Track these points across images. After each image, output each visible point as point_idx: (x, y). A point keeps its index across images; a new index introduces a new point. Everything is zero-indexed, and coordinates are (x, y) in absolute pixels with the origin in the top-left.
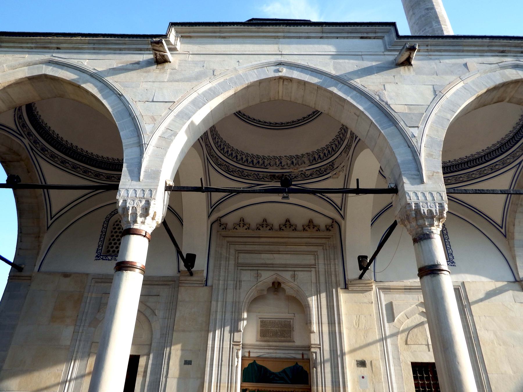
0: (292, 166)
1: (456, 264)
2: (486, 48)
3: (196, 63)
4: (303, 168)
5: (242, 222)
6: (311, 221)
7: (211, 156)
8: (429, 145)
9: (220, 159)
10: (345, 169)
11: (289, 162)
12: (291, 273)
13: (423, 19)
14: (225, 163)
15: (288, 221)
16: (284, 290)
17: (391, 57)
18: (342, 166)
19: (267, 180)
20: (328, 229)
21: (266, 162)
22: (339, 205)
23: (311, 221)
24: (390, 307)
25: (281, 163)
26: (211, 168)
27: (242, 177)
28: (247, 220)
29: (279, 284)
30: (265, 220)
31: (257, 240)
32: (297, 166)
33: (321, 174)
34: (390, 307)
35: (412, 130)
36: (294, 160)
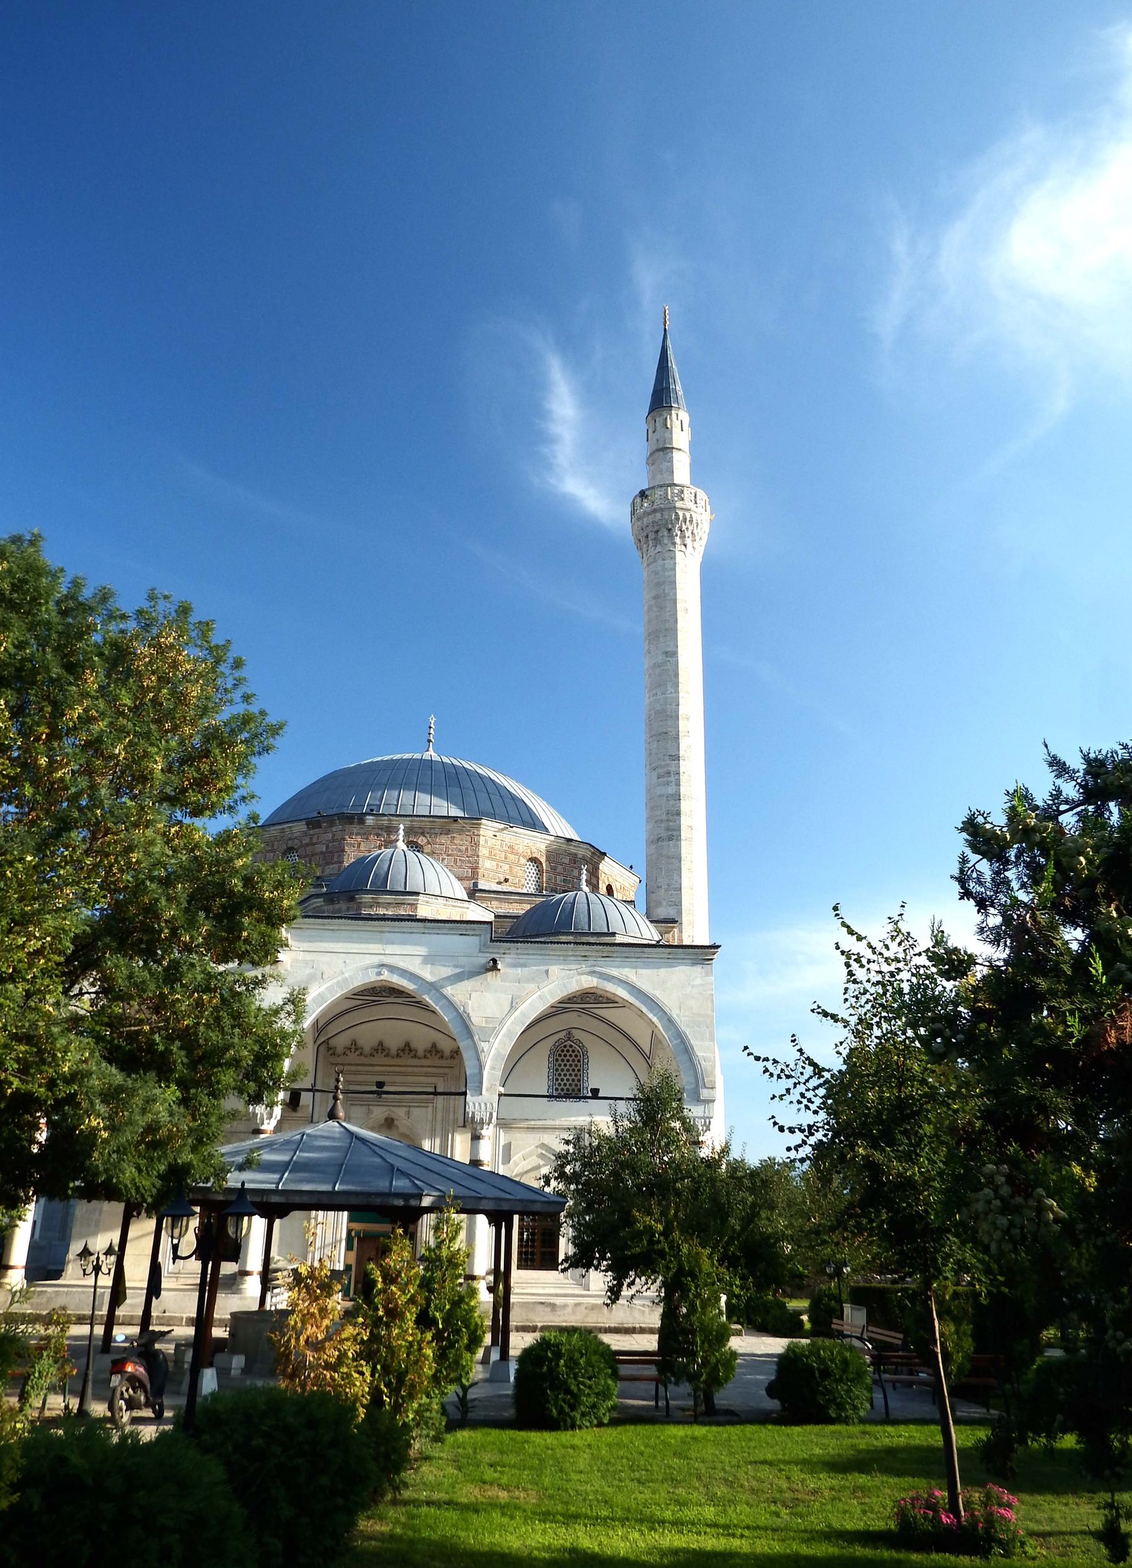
2: (570, 953)
3: (306, 962)
5: (354, 1047)
6: (434, 1046)
8: (496, 1058)
12: (405, 1109)
13: (658, 670)
15: (407, 1044)
16: (397, 1127)
17: (484, 959)
20: (452, 1057)
23: (434, 1046)
24: (508, 1148)
28: (360, 1042)
29: (392, 1120)
30: (381, 1044)
31: (370, 1068)
34: (508, 1148)
35: (483, 1044)
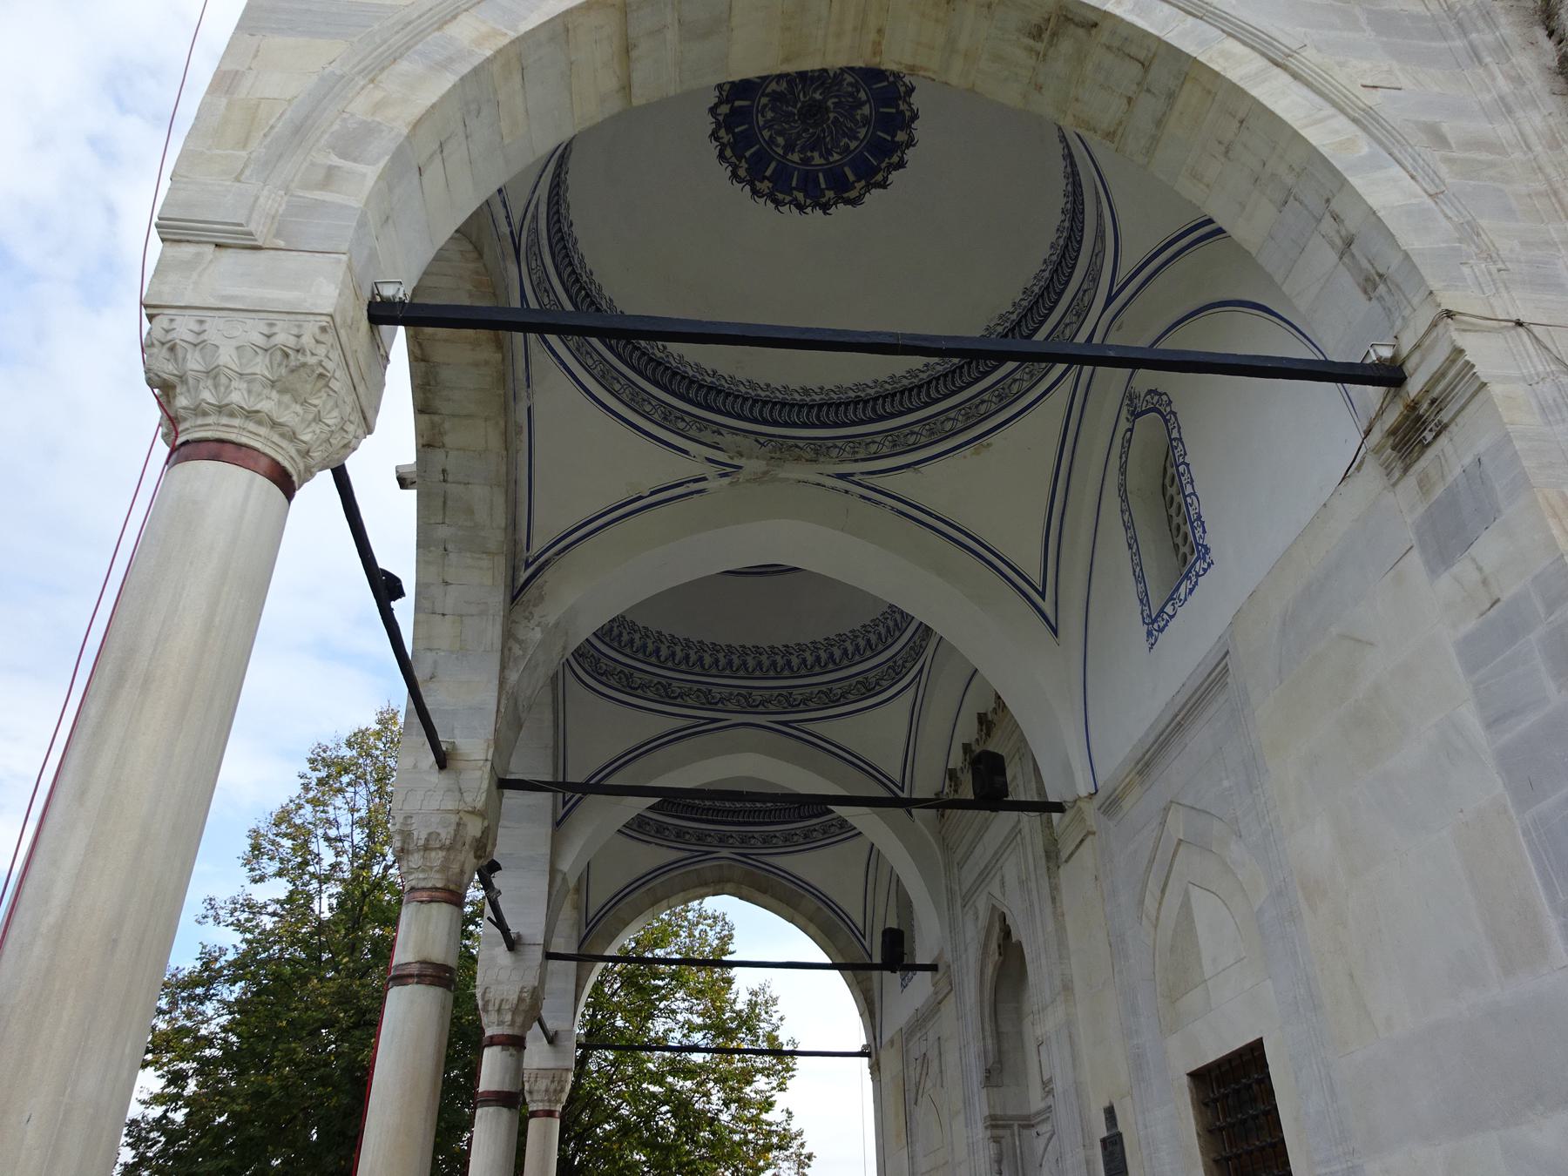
1: (1213, 555)
7: (793, 706)
26: (810, 727)
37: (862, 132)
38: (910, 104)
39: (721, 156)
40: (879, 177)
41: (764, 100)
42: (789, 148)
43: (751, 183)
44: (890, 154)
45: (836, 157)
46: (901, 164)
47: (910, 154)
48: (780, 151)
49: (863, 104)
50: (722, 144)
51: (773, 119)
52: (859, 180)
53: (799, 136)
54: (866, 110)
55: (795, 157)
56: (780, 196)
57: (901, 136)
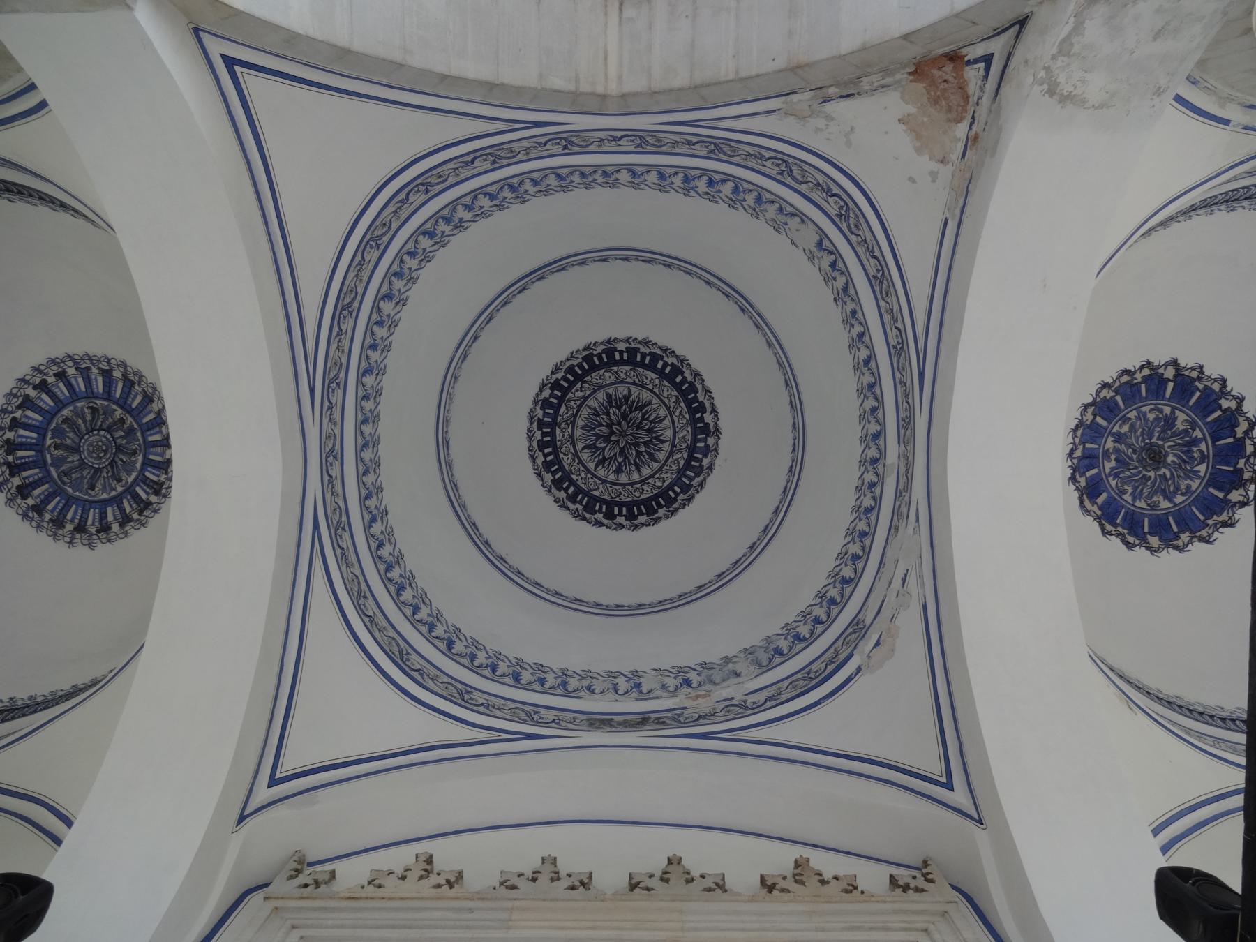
0: (685, 690)
4: (732, 691)
9: (371, 601)
10: (912, 580)
11: (671, 683)
14: (392, 633)
18: (897, 583)
19: (570, 726)
20: (906, 888)
21: (573, 683)
22: (934, 768)
25: (638, 686)
27: (460, 702)
32: (708, 687)
33: (812, 679)
36: (693, 676)
37: (1141, 504)
38: (1190, 542)
39: (1126, 372)
40: (1109, 527)
41: (1167, 410)
42: (1119, 438)
43: (1093, 404)
44: (1133, 532)
45: (1113, 483)
46: (1129, 546)
47: (1141, 552)
48: (1114, 430)
49: (1170, 500)
50: (1135, 372)
51: (1146, 419)
52: (1100, 508)
53: (1129, 446)
54: (1165, 504)
55: (1110, 444)
56: (1079, 433)
57: (1154, 541)
